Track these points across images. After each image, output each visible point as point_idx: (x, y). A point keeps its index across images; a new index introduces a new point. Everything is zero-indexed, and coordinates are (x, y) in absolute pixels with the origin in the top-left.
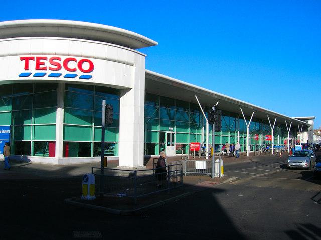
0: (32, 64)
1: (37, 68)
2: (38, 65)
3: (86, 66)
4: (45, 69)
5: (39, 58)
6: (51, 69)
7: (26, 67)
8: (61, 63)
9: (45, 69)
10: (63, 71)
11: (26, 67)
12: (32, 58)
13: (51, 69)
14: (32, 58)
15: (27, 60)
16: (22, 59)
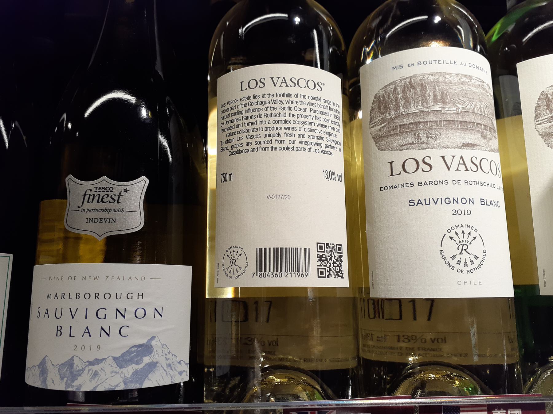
0: (98, 189)
1: (99, 190)
2: (99, 189)
3: (111, 189)
4: (101, 190)
5: (99, 187)
6: (102, 190)
7: (96, 189)
8: (105, 188)
9: (101, 190)
10: (105, 190)
11: (96, 189)
12: (98, 187)
13: (102, 190)
14: (98, 187)
15: (96, 188)
16: (95, 187)
